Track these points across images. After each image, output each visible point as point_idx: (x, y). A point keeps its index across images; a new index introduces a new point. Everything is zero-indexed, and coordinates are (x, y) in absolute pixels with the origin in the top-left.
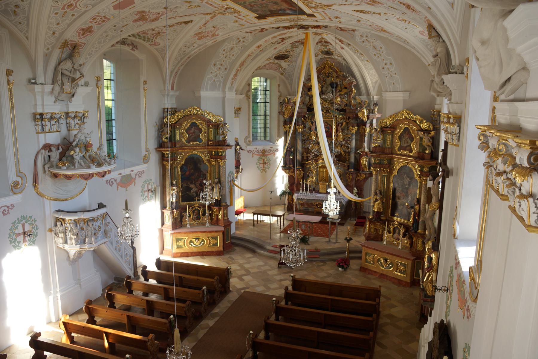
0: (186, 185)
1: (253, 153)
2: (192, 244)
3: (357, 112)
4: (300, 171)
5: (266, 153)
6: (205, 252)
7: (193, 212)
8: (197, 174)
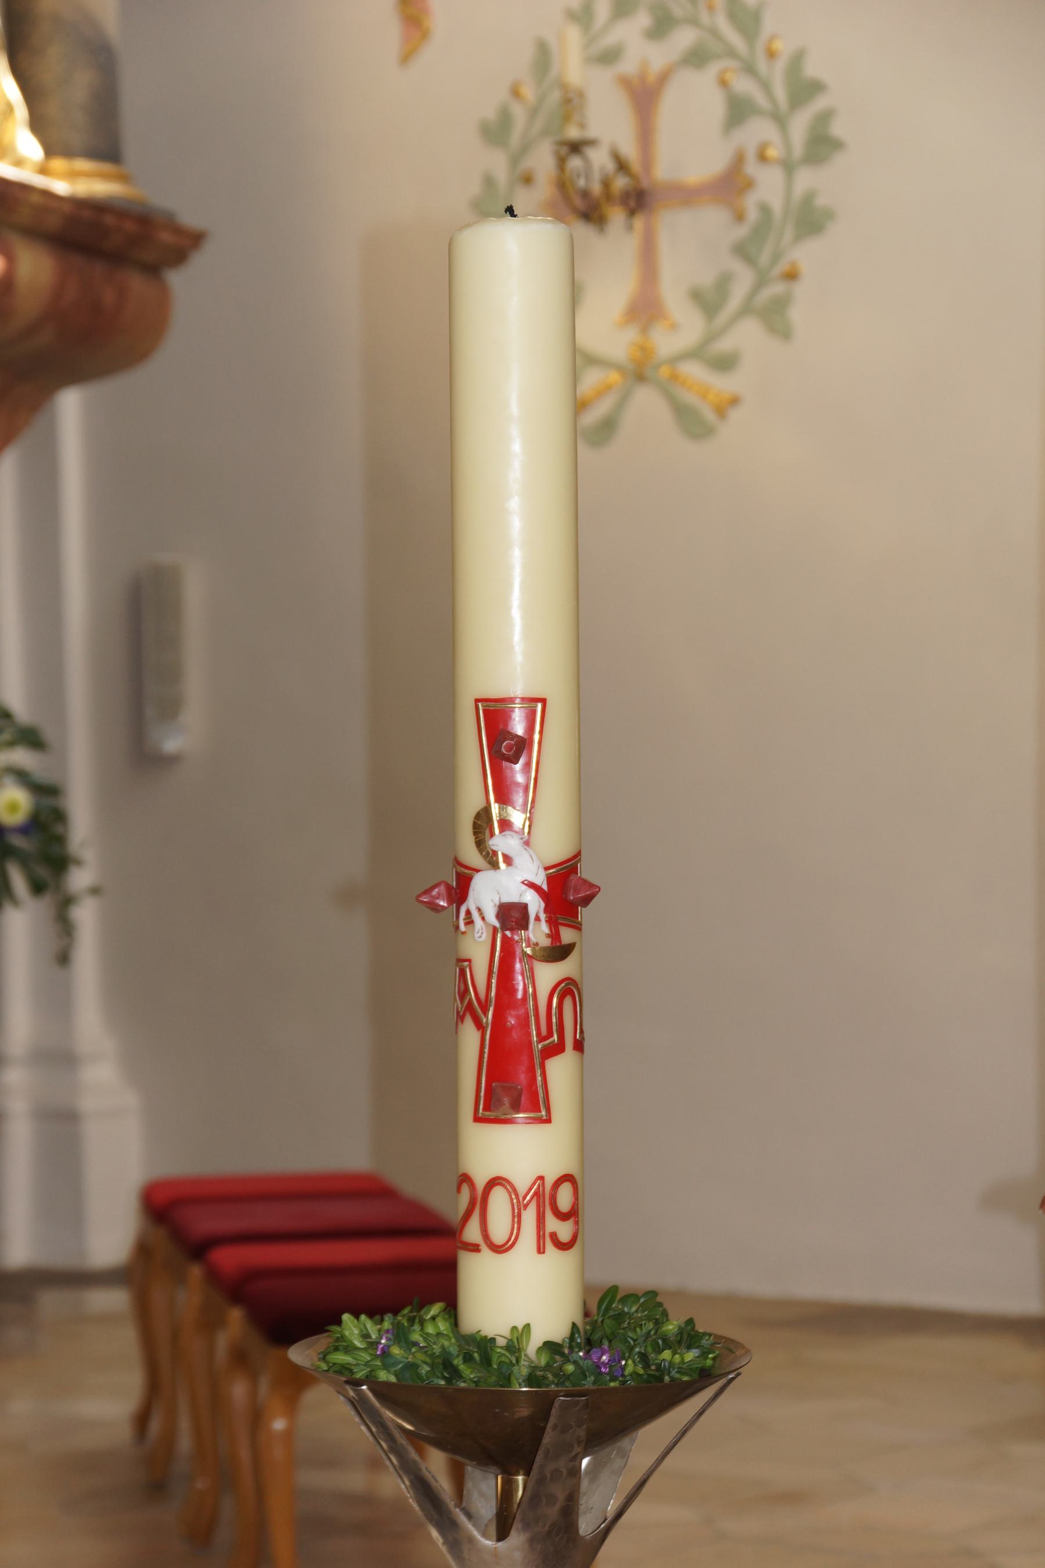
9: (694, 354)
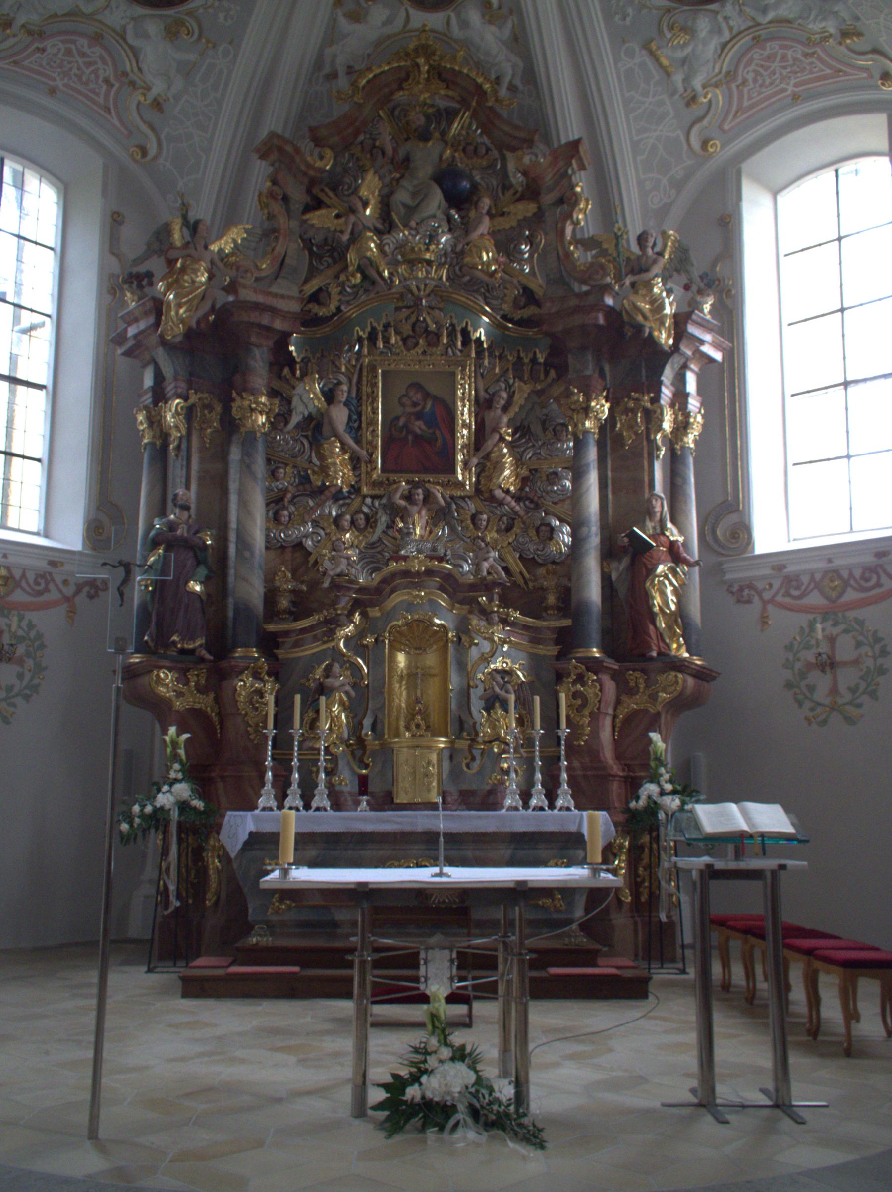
3: (609, 301)
4: (256, 676)
5: (19, 596)
9: (850, 703)
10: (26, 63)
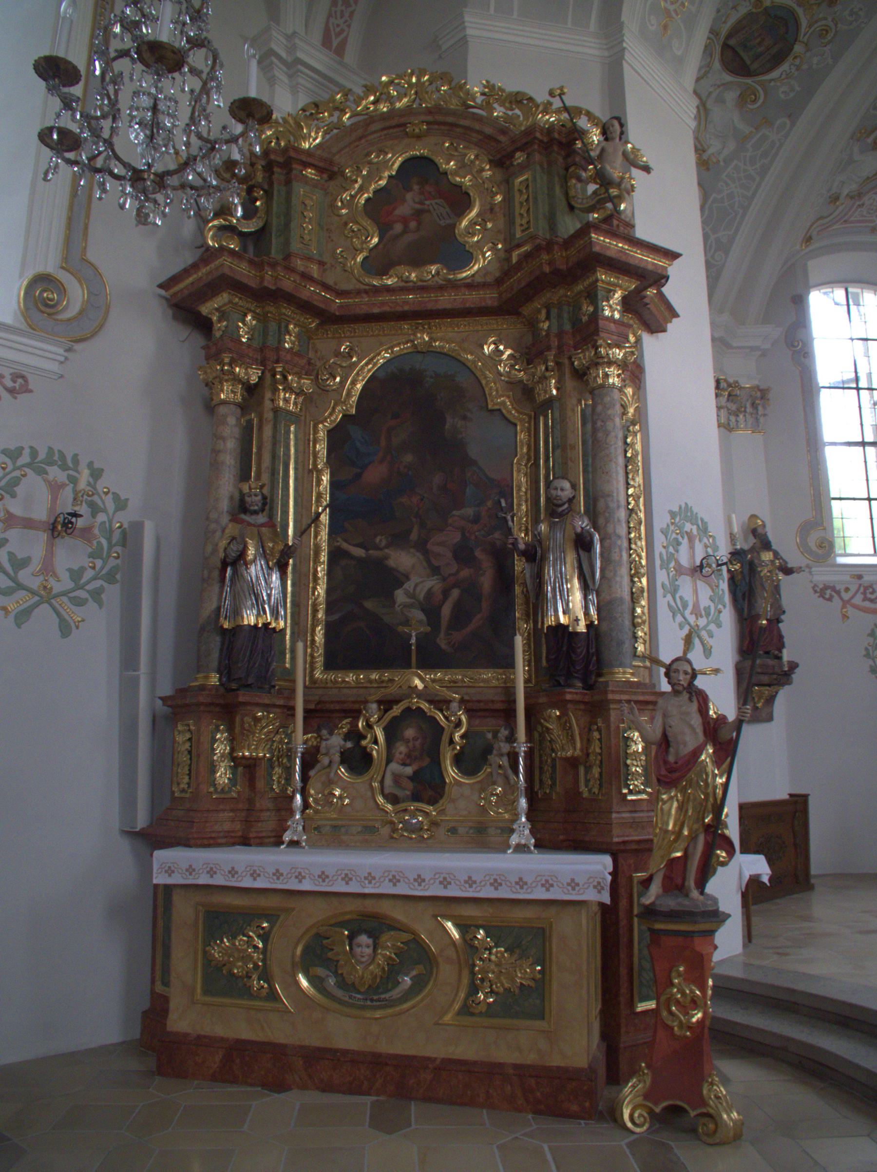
0: (359, 552)
1: (845, 603)
2: (320, 971)
6: (425, 1061)
7: (391, 733)
8: (437, 479)
10: (852, 219)
